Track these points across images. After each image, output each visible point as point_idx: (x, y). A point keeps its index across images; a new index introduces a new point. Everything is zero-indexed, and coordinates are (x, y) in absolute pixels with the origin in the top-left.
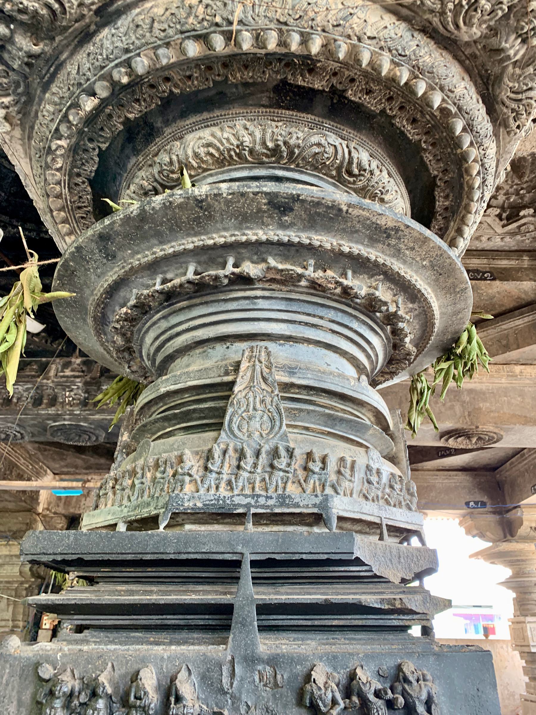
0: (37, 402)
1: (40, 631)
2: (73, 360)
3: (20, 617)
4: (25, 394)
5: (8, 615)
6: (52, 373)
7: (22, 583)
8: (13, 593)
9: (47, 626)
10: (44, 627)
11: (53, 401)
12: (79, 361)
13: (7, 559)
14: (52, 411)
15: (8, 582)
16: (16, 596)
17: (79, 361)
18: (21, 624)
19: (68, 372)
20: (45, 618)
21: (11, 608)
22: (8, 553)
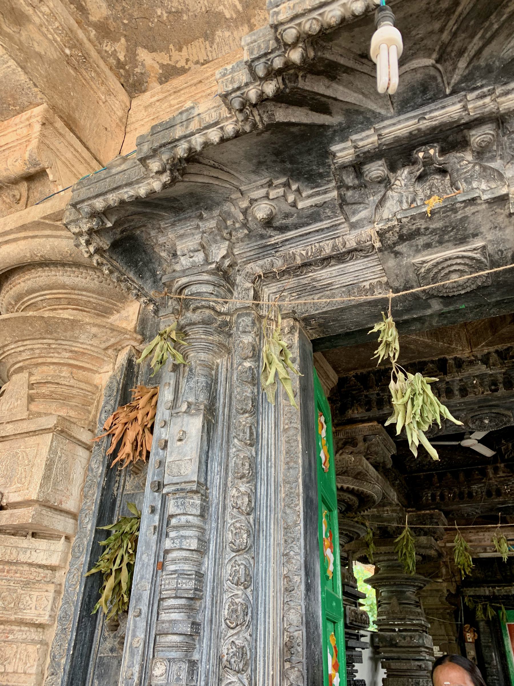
0: (489, 494)
1: (466, 644)
2: (498, 465)
3: (451, 633)
4: (479, 490)
5: (443, 632)
6: (491, 476)
7: (446, 609)
8: (441, 616)
9: (471, 640)
10: (469, 641)
11: (499, 493)
12: (502, 465)
13: (429, 593)
14: (501, 499)
15: (437, 609)
16: (444, 619)
17: (502, 465)
18: (454, 638)
19: (501, 474)
20: (468, 634)
21: (443, 627)
22: (430, 588)
